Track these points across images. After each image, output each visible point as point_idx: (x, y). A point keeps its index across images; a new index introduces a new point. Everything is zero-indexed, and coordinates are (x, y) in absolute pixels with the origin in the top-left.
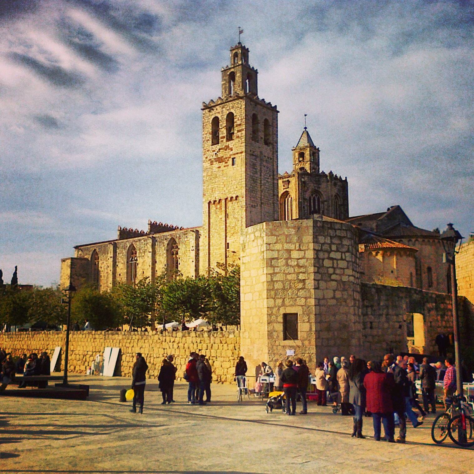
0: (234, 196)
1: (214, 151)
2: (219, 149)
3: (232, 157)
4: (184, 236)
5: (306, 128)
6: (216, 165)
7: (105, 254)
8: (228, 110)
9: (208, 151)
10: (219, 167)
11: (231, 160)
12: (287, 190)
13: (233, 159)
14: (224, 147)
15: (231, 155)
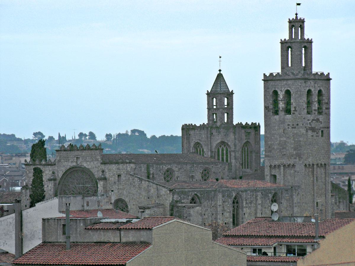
0: (323, 163)
1: (309, 120)
2: (313, 120)
3: (322, 129)
4: (285, 192)
5: (220, 71)
6: (310, 133)
7: (209, 201)
8: (319, 87)
9: (304, 118)
10: (312, 136)
11: (320, 131)
12: (249, 140)
13: (322, 131)
14: (316, 119)
15: (321, 128)
